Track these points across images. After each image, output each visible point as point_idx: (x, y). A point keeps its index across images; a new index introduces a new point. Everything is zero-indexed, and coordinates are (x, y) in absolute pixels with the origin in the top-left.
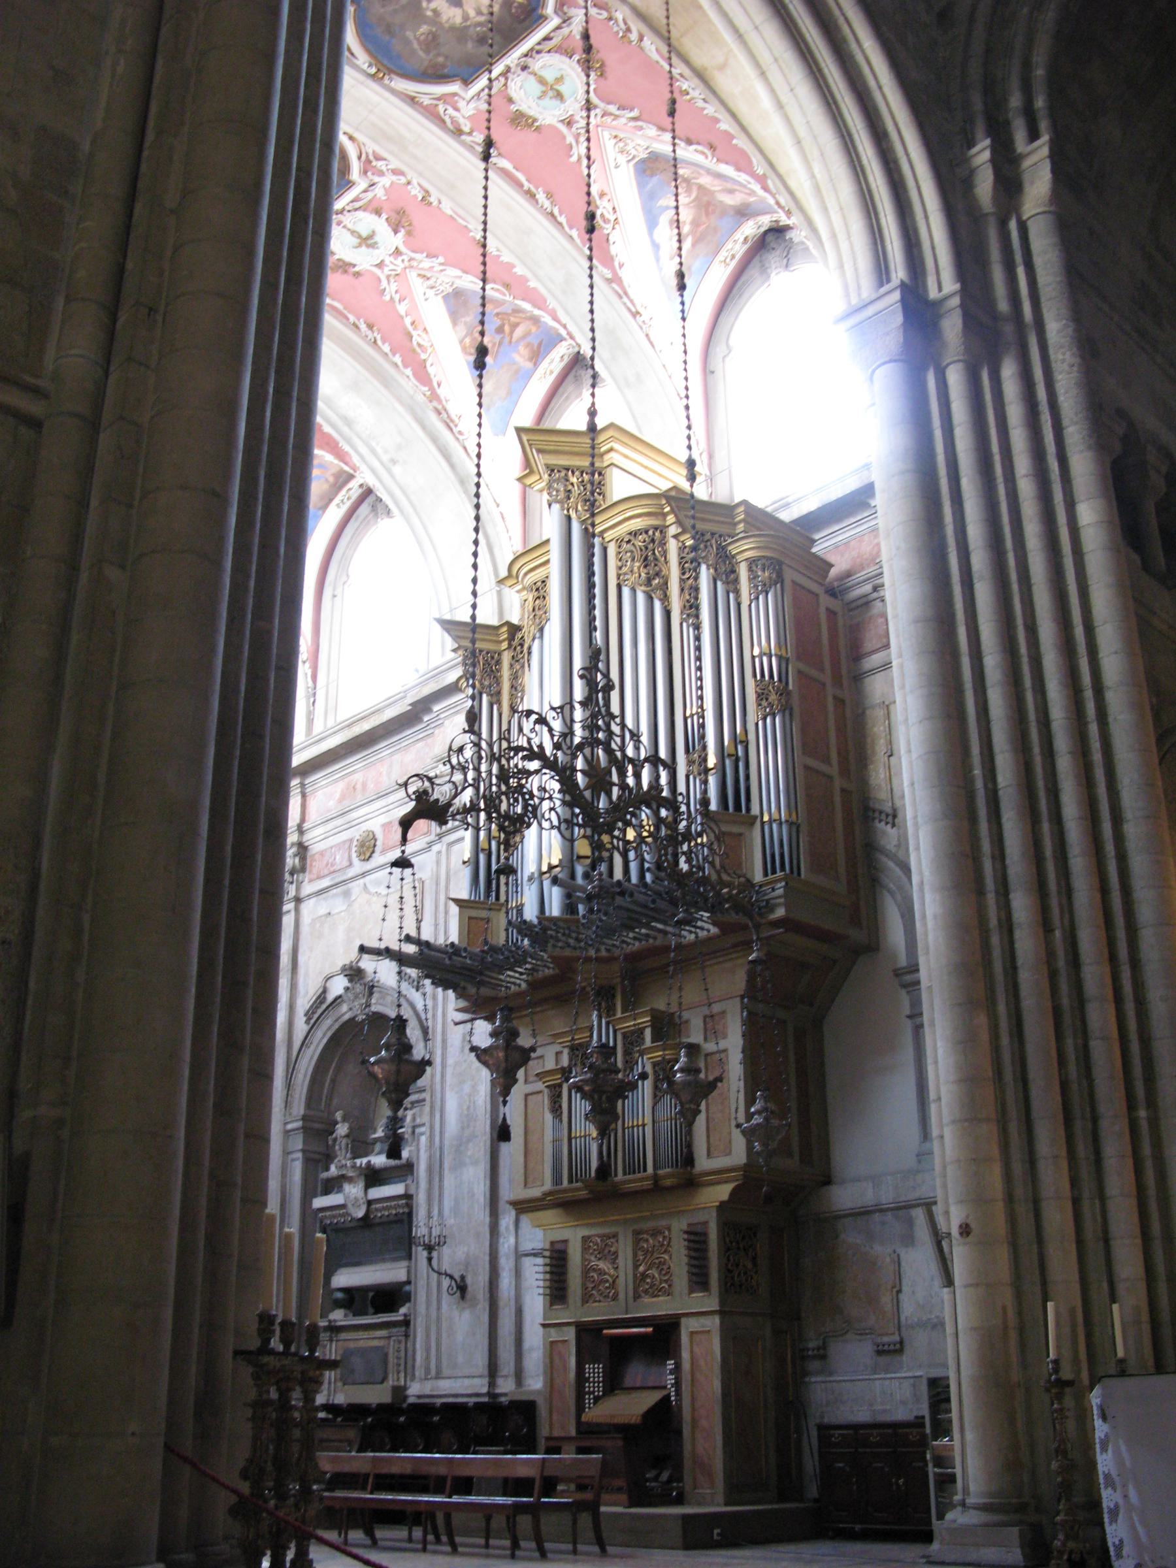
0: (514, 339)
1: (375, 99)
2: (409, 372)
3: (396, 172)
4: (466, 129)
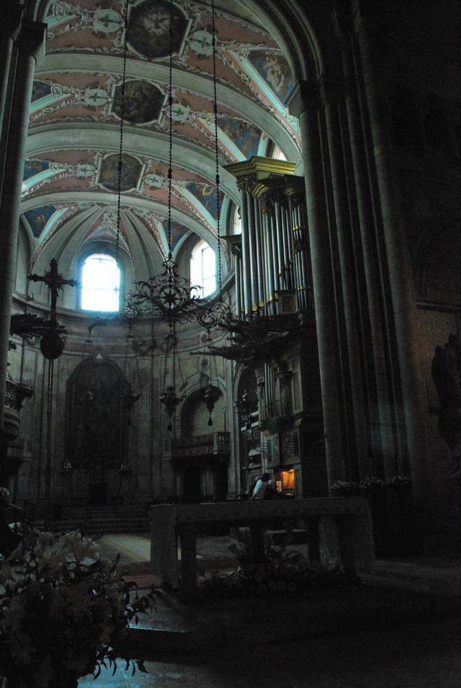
1: (153, 67)
4: (187, 66)
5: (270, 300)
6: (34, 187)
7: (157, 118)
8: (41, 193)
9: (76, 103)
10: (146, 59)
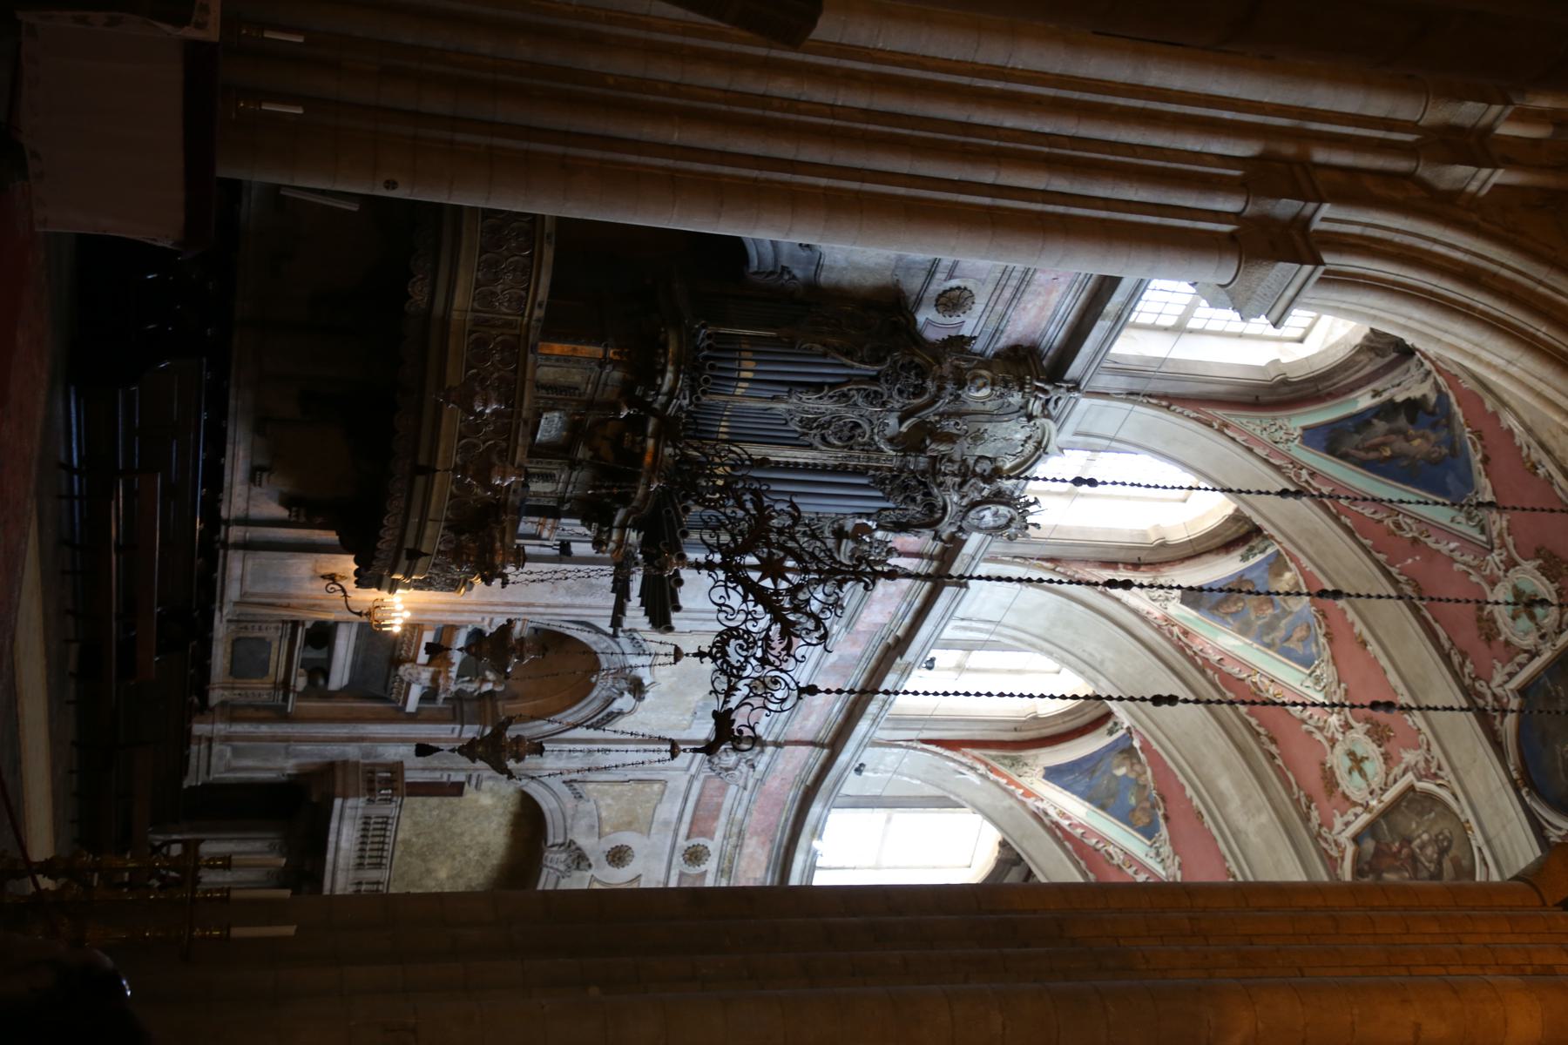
6: (1088, 831)
8: (1083, 863)
10: (1515, 775)
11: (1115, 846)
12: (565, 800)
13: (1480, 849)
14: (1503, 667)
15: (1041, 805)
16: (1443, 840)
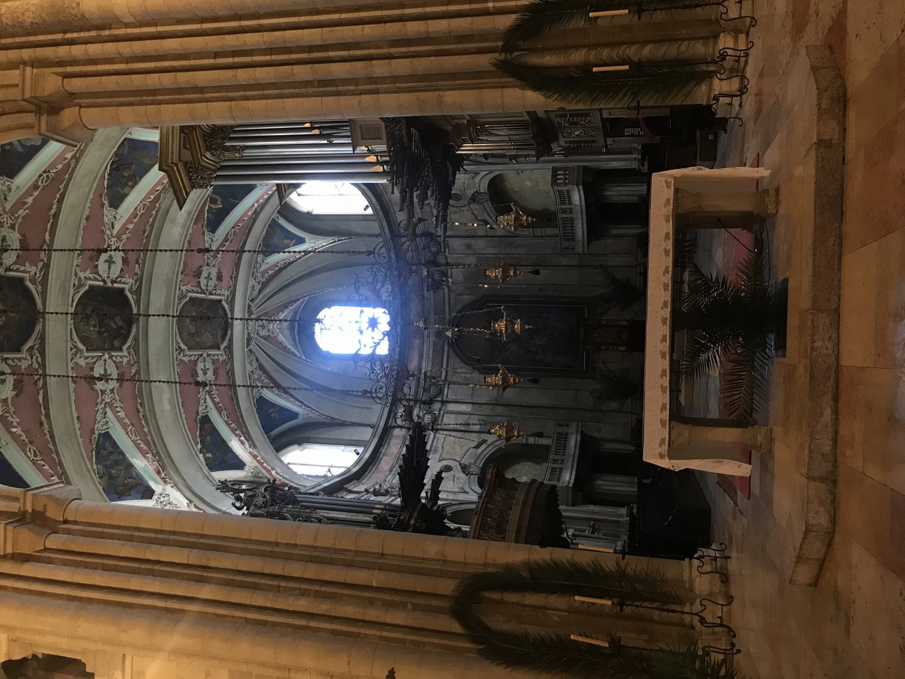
0: (118, 159)
2: (157, 205)
3: (76, 275)
4: (42, 263)
5: (366, 149)
6: (233, 431)
7: (122, 290)
9: (117, 398)
10: (41, 320)
11: (224, 419)
12: (469, 488)
13: (72, 306)
14: (21, 366)
15: (252, 450)
16: (85, 322)
